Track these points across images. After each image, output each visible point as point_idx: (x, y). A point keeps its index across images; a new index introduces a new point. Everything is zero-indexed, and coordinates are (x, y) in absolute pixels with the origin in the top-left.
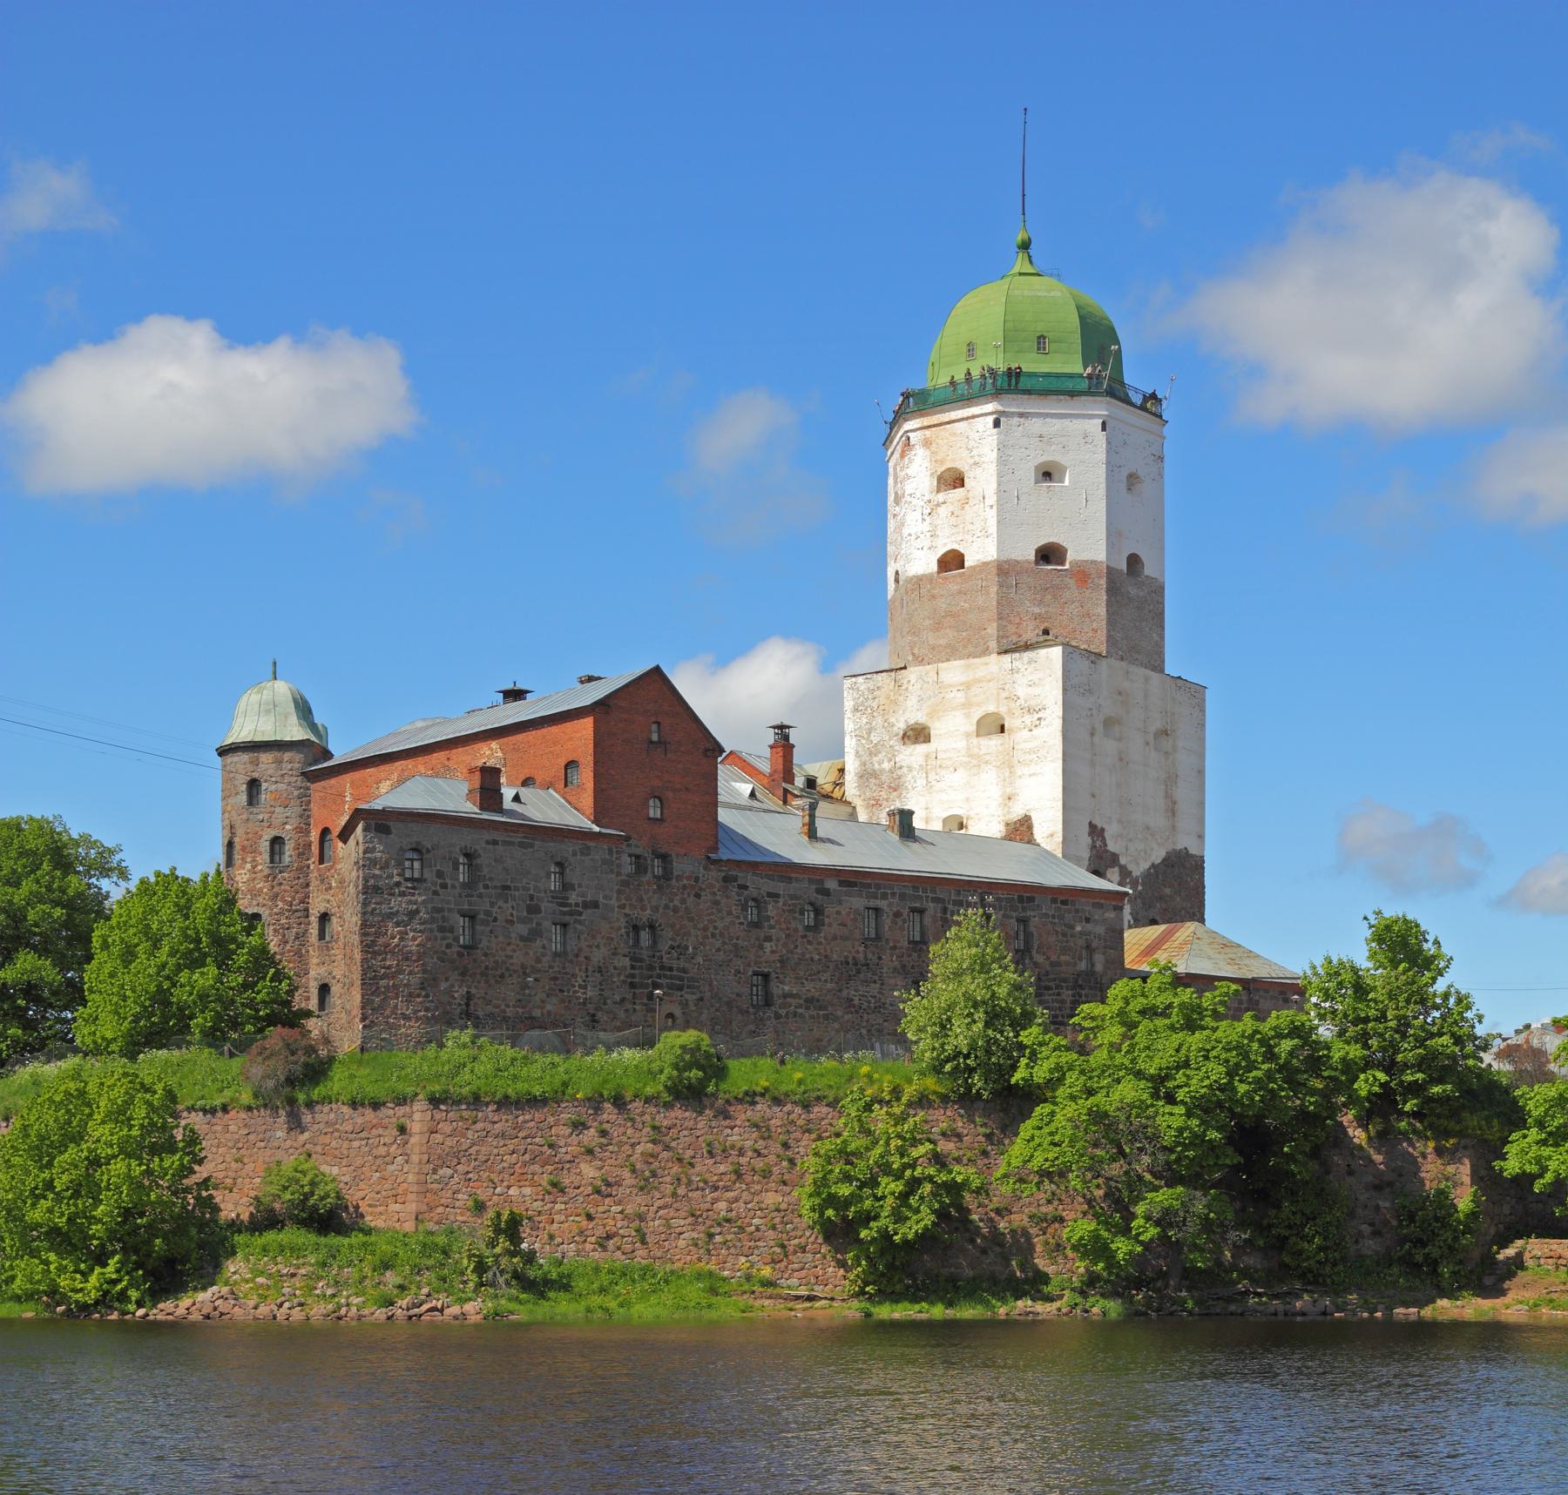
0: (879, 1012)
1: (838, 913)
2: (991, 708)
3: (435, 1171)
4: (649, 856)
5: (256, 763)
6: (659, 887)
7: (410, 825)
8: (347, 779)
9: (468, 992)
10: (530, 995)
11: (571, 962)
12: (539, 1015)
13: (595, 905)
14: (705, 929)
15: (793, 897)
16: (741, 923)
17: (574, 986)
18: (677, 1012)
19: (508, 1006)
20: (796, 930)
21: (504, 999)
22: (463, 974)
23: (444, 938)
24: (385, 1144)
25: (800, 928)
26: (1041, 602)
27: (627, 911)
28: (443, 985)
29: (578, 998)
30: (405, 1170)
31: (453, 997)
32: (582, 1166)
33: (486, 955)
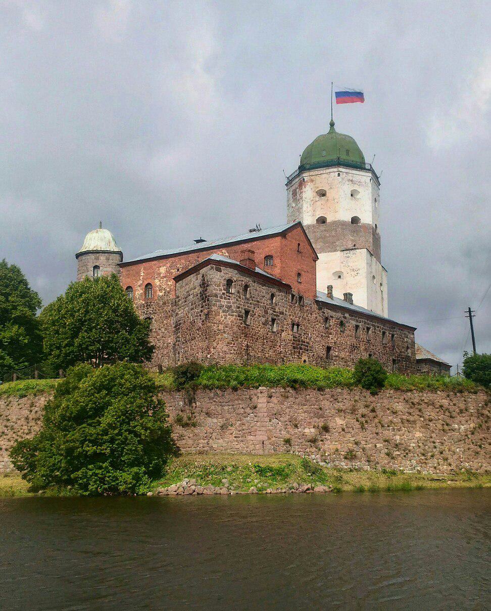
1: (349, 326)
2: (338, 269)
3: (270, 421)
8: (142, 267)
18: (307, 360)
19: (259, 352)
27: (291, 317)
29: (278, 351)
33: (252, 329)
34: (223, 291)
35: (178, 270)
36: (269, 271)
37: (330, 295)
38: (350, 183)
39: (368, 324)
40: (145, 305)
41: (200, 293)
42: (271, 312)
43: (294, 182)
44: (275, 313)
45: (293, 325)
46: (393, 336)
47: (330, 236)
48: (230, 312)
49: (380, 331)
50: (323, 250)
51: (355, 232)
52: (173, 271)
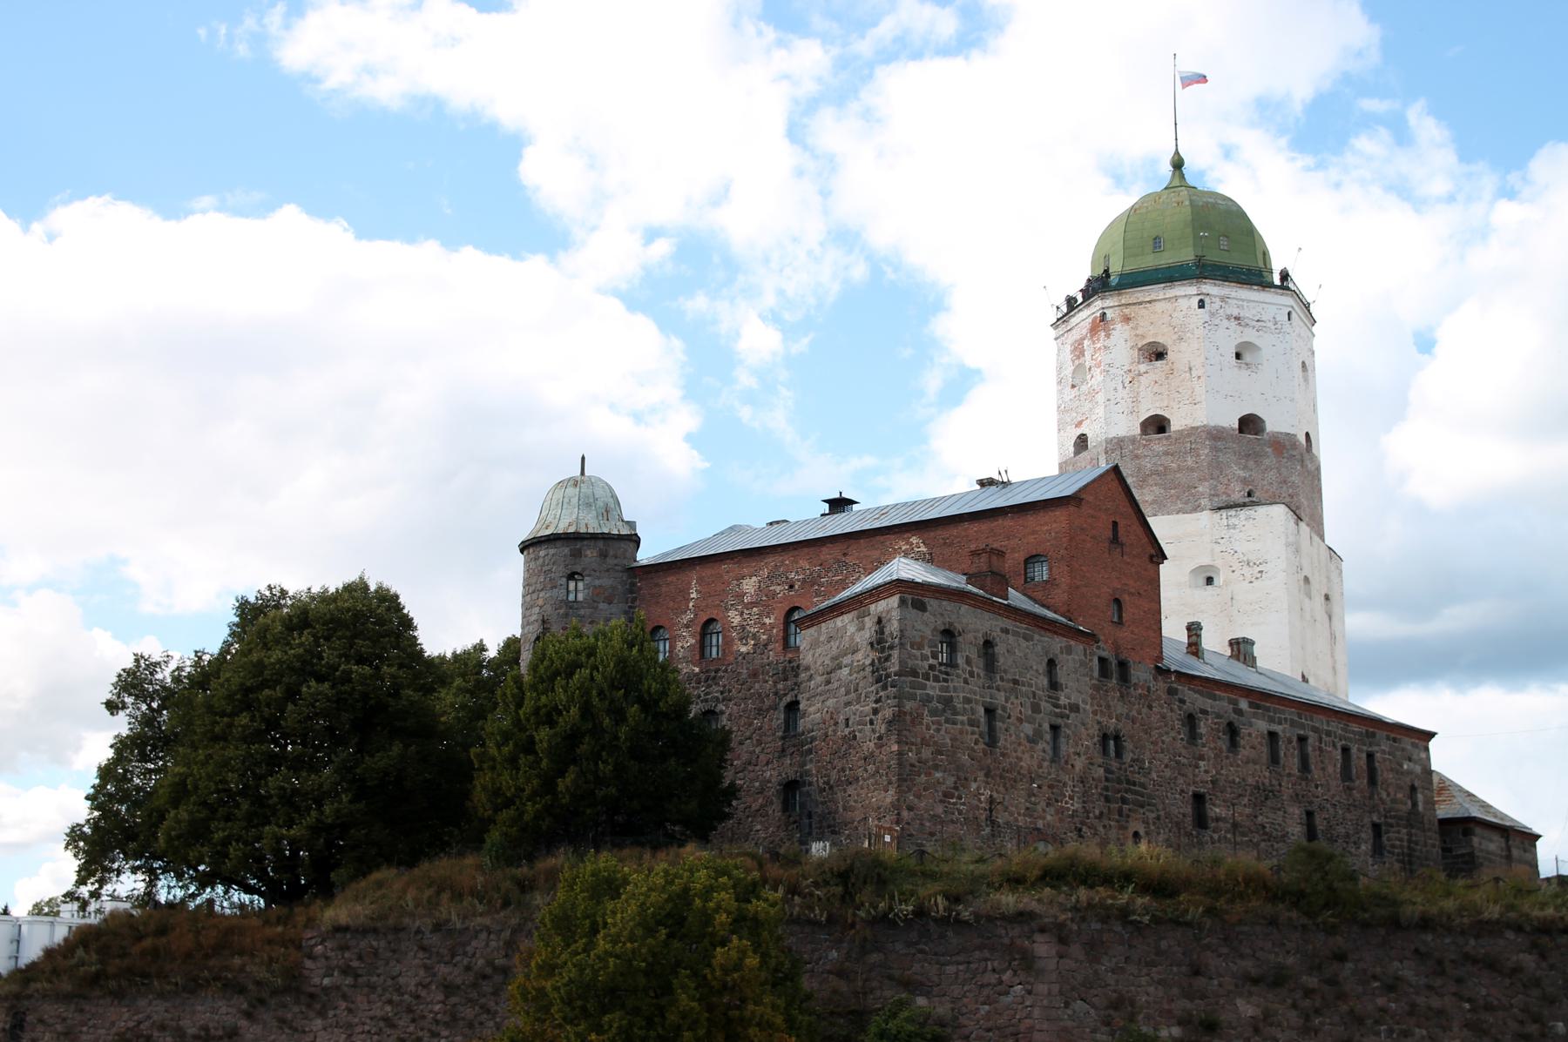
0: (1284, 841)
1: (1250, 735)
2: (1206, 561)
3: (1067, 1005)
4: (1114, 663)
5: (577, 554)
6: (1122, 696)
7: (944, 603)
9: (991, 796)
10: (1035, 804)
11: (1062, 769)
12: (1041, 827)
13: (1075, 708)
14: (1154, 743)
15: (1218, 716)
16: (1182, 739)
17: (1065, 796)
18: (1142, 832)
19: (1019, 814)
20: (1221, 750)
21: (1017, 807)
22: (987, 775)
23: (973, 733)
24: (994, 970)
25: (1224, 748)
26: (1245, 468)
27: (1098, 717)
28: (974, 786)
29: (1068, 809)
30: (1028, 1003)
31: (979, 800)
32: (1239, 1002)
33: (1003, 755)
34: (931, 661)
35: (791, 587)
36: (1039, 595)
37: (1194, 648)
38: (1233, 323)
39: (1302, 726)
40: (703, 677)
41: (872, 664)
42: (1049, 707)
43: (1074, 321)
44: (1057, 710)
45: (1105, 738)
46: (1370, 756)
47: (1180, 469)
48: (948, 714)
49: (1334, 746)
50: (1161, 507)
51: (1253, 456)
52: (778, 589)
